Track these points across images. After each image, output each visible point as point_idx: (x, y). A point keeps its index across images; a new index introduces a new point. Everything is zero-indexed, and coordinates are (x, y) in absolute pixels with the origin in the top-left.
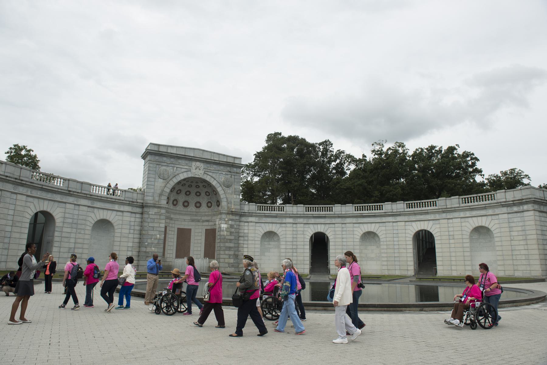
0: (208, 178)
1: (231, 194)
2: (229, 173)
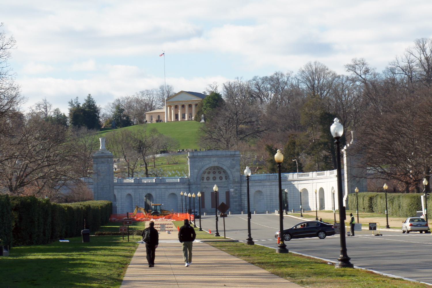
0: (220, 166)
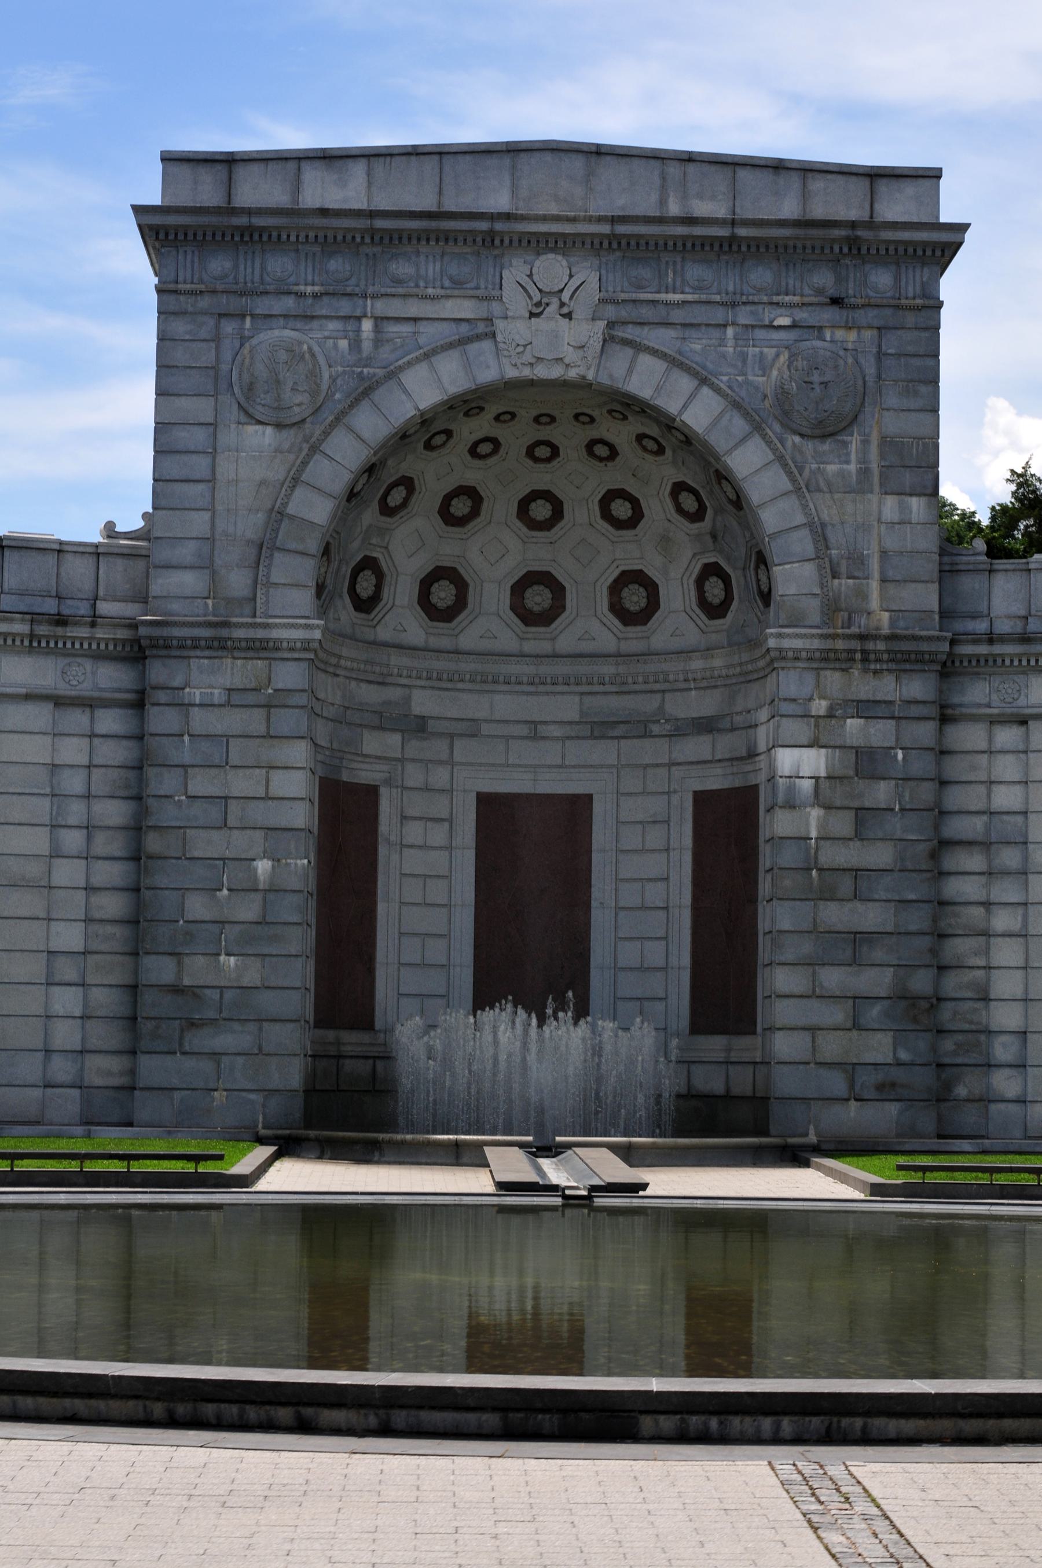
1: (861, 485)
2: (829, 315)
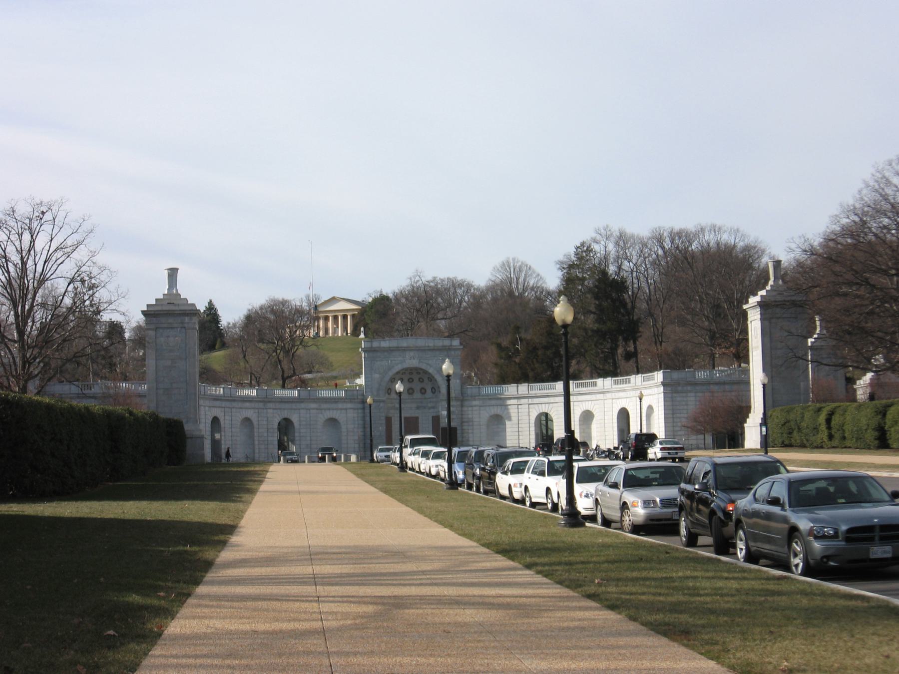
0: (424, 366)
